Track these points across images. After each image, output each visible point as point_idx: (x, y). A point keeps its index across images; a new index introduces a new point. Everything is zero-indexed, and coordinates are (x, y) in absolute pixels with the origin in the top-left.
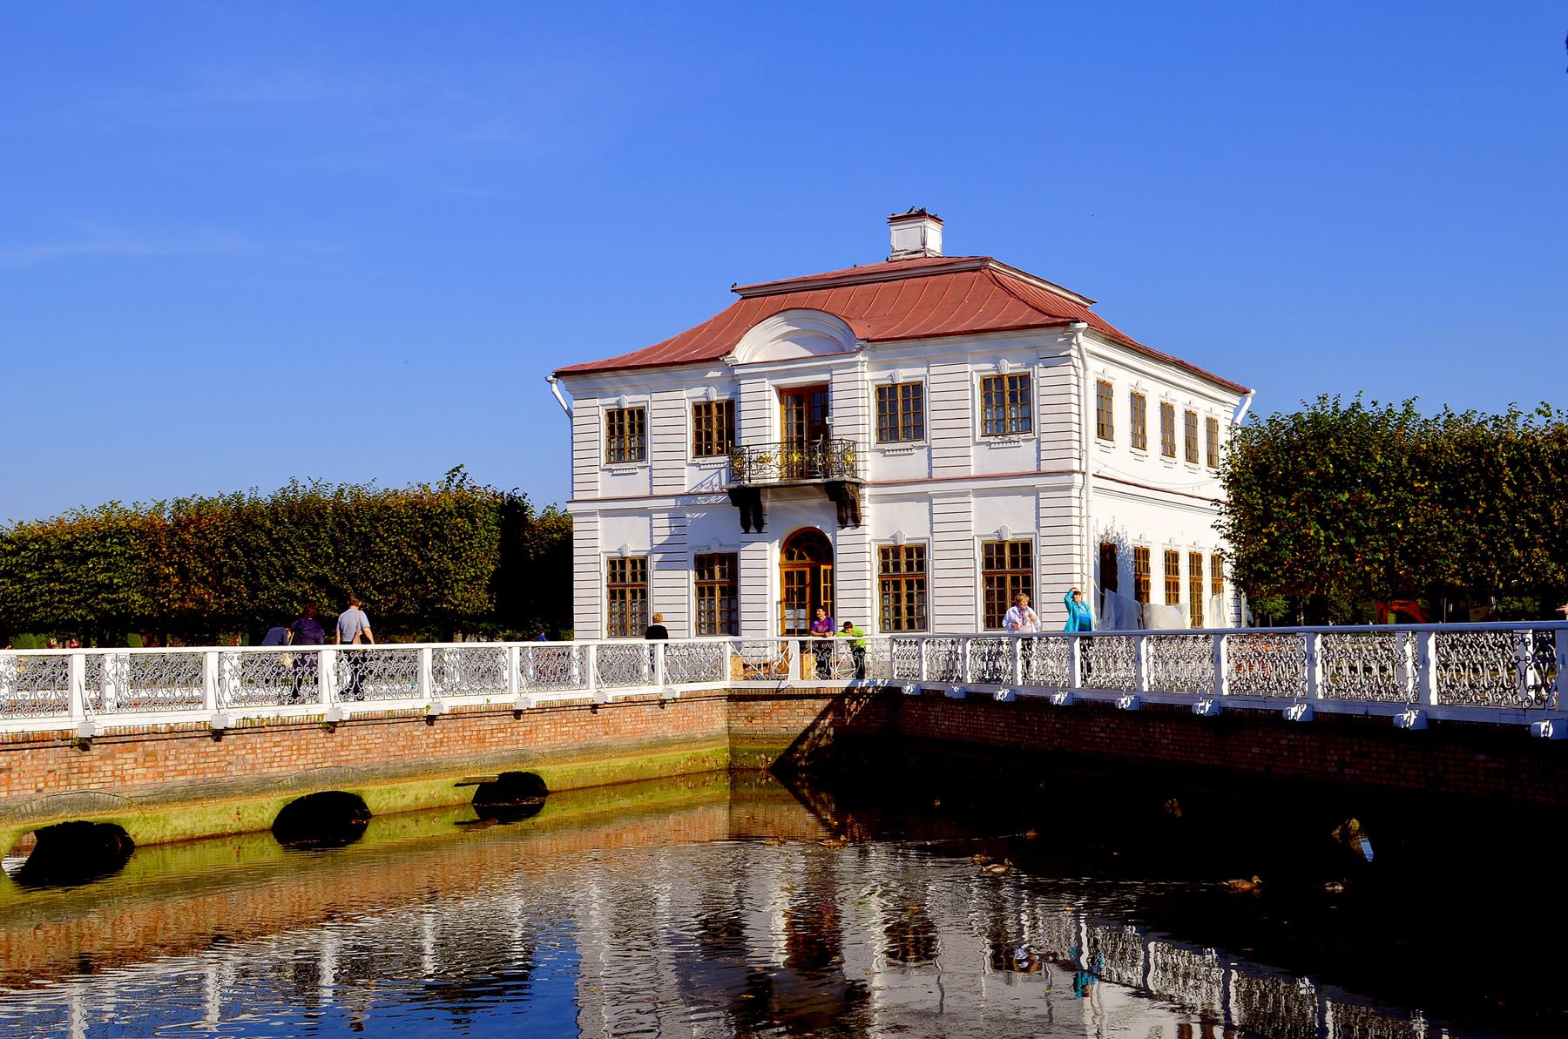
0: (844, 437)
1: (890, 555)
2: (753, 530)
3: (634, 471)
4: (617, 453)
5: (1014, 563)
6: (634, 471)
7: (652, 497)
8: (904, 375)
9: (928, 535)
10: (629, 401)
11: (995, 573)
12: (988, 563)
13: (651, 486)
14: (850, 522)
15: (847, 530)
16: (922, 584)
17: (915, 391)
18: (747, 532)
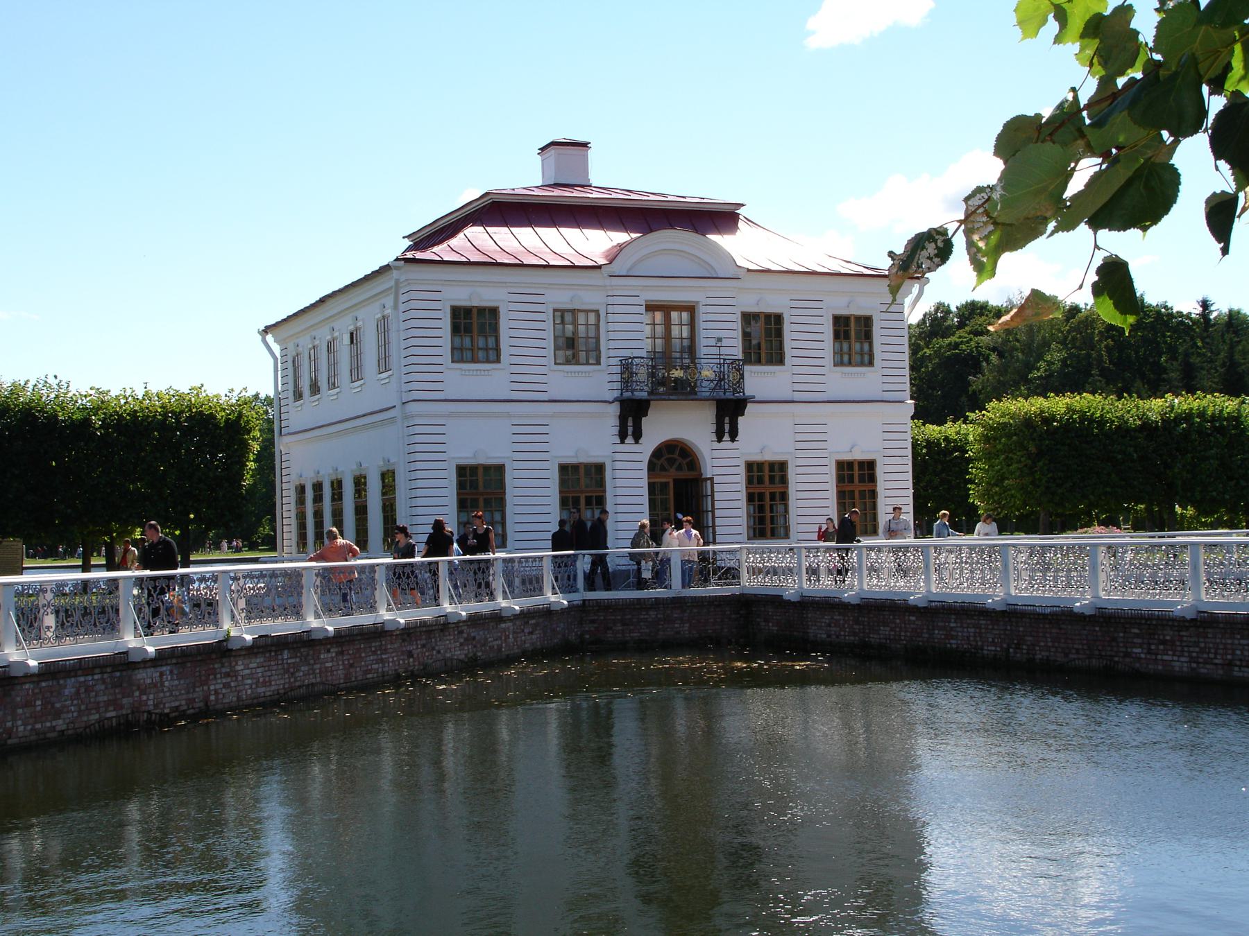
0: (726, 357)
2: (630, 440)
5: (862, 480)
12: (840, 479)
14: (727, 437)
18: (622, 442)
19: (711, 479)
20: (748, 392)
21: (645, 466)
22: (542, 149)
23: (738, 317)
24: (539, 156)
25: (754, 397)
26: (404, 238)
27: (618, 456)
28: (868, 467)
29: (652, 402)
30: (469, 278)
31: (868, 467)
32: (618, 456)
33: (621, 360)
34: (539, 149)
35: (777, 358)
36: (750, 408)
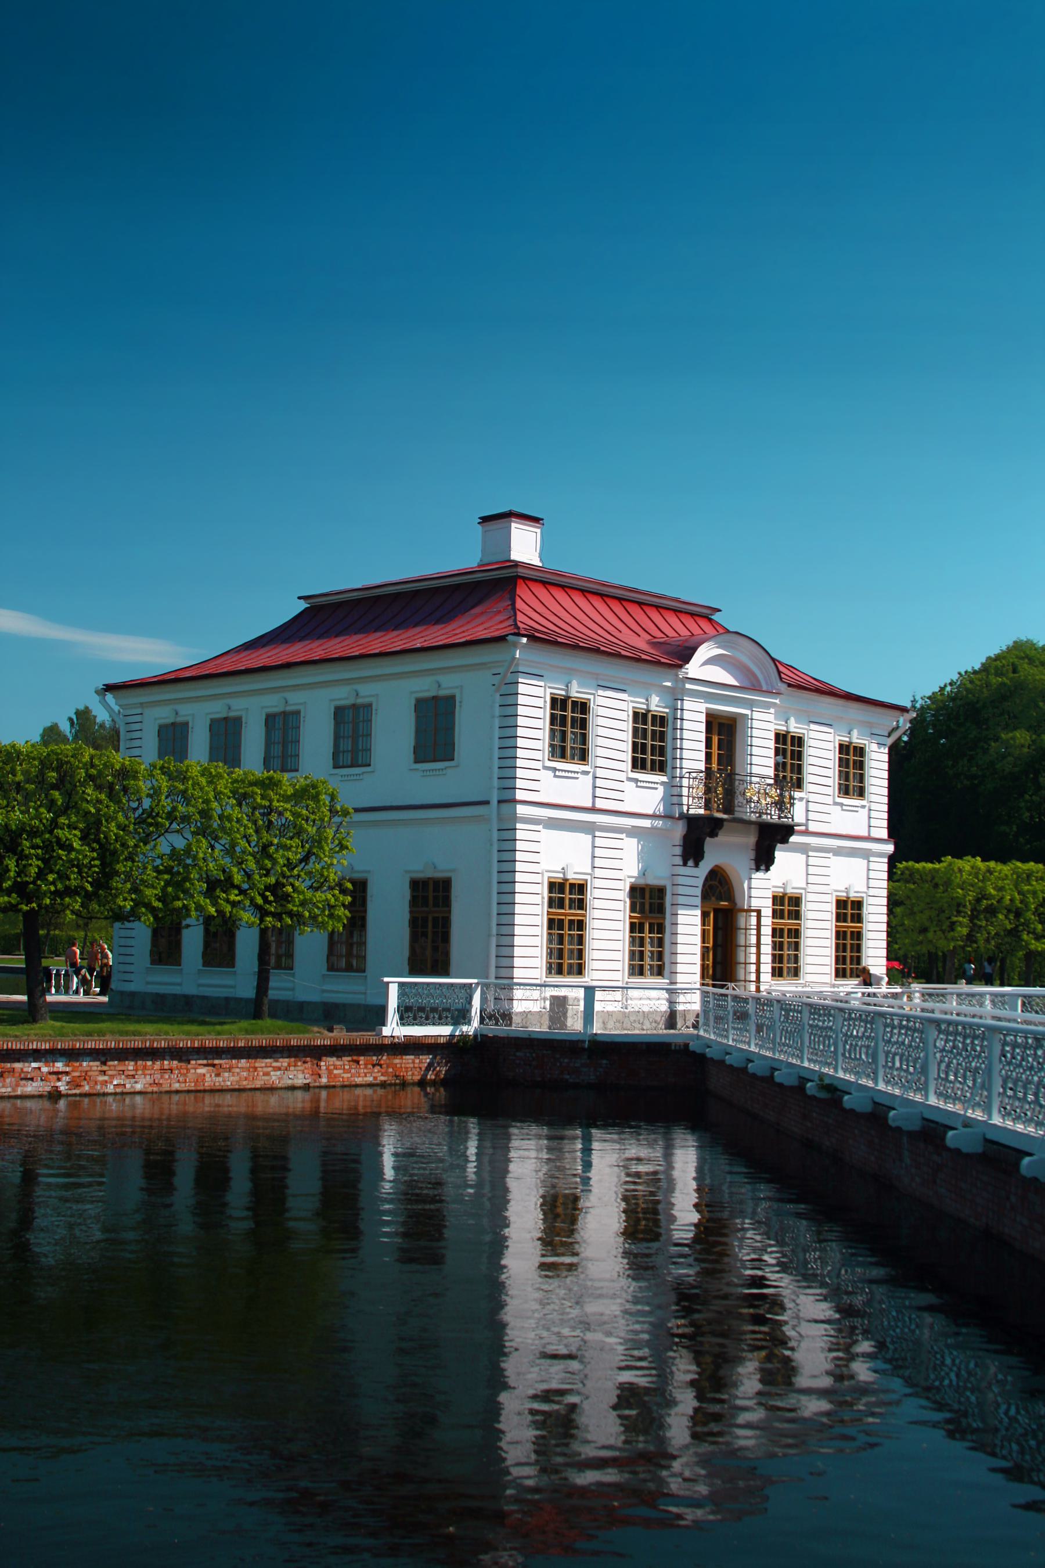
1: (778, 900)
2: (690, 863)
3: (576, 775)
4: (559, 751)
6: (576, 775)
7: (593, 810)
10: (577, 692)
13: (594, 797)
15: (760, 875)
16: (796, 933)
17: (799, 741)
18: (685, 864)
21: (698, 892)
22: (485, 520)
23: (772, 736)
24: (480, 527)
26: (300, 598)
27: (681, 880)
28: (858, 905)
30: (485, 659)
31: (858, 905)
32: (681, 880)
33: (690, 773)
34: (480, 518)
36: (793, 839)
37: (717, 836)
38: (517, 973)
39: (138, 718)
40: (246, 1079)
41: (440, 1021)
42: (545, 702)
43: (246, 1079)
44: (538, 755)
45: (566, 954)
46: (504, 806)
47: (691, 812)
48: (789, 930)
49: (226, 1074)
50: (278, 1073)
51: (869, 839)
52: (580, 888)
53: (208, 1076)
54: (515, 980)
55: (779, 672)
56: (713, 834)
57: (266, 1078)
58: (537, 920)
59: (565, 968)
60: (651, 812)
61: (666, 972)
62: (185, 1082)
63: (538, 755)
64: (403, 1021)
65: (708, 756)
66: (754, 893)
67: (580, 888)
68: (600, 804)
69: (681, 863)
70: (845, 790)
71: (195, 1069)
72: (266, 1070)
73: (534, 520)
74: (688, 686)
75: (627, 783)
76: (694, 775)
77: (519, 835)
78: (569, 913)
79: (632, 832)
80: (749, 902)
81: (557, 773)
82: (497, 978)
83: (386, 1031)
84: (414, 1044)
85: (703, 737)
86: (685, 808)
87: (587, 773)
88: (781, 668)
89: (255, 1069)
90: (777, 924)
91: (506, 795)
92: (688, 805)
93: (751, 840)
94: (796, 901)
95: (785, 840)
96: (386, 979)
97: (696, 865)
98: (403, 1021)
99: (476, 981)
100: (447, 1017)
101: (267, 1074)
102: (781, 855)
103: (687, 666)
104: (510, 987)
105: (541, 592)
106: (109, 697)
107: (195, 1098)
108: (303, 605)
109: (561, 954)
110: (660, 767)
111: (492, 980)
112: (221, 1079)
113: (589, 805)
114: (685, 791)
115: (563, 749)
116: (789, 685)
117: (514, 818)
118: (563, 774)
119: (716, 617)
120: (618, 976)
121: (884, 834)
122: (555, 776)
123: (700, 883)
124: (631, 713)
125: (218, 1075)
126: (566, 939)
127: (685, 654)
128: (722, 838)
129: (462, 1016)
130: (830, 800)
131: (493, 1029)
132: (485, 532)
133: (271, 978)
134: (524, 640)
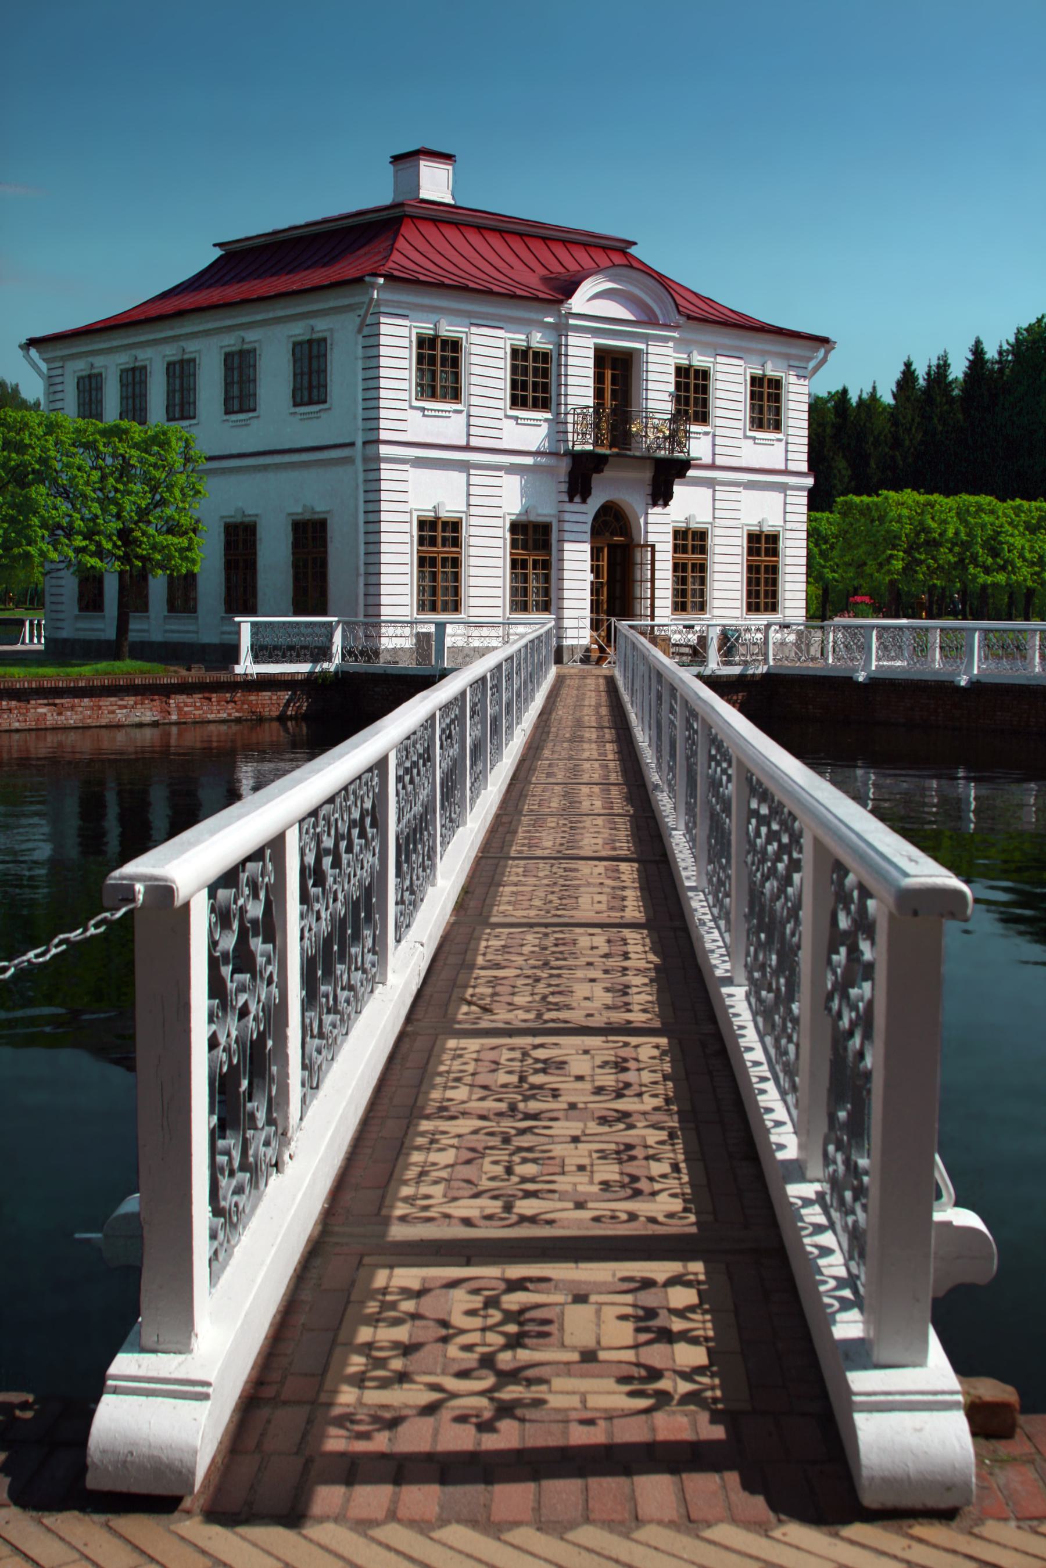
1: (680, 535)
2: (577, 499)
3: (447, 414)
6: (447, 414)
7: (468, 448)
8: (699, 360)
9: (782, 524)
10: (448, 329)
11: (438, 553)
13: (469, 435)
17: (704, 375)
18: (571, 500)
19: (653, 547)
20: (693, 454)
21: (588, 528)
22: (397, 159)
23: (672, 370)
24: (391, 167)
25: (700, 459)
26: (215, 245)
28: (774, 538)
29: (610, 459)
31: (774, 538)
35: (703, 418)
36: (691, 473)
37: (602, 471)
38: (384, 611)
39: (59, 372)
40: (90, 717)
41: (298, 659)
42: (411, 341)
43: (90, 717)
44: (405, 395)
45: (440, 592)
46: (368, 447)
47: (578, 448)
48: (693, 564)
49: (69, 713)
50: (124, 711)
51: (786, 472)
52: (455, 526)
53: (49, 715)
54: (383, 618)
55: (677, 305)
56: (600, 471)
57: (111, 716)
58: (407, 559)
59: (439, 604)
60: (534, 449)
61: (553, 608)
62: (26, 721)
63: (405, 395)
64: (257, 659)
65: (599, 394)
66: (650, 528)
67: (455, 526)
68: (474, 442)
69: (567, 499)
70: (758, 423)
71: (36, 708)
72: (110, 708)
73: (446, 157)
74: (572, 322)
75: (505, 420)
76: (579, 411)
77: (384, 475)
78: (441, 551)
79: (512, 469)
80: (646, 537)
81: (426, 413)
82: (365, 616)
83: (239, 669)
84: (270, 681)
85: (591, 373)
86: (570, 444)
87: (460, 412)
88: (679, 300)
89: (100, 707)
90: (679, 558)
91: (371, 437)
92: (573, 442)
93: (648, 475)
94: (701, 535)
95: (682, 475)
96: (237, 619)
97: (584, 501)
98: (257, 659)
99: (336, 619)
100: (305, 655)
101: (113, 712)
102: (679, 490)
103: (570, 301)
104: (378, 625)
105: (430, 231)
106: (33, 352)
107: (37, 737)
108: (218, 253)
109: (434, 591)
110: (543, 404)
111: (361, 618)
112: (63, 718)
113: (464, 443)
114: (570, 428)
115: (433, 388)
116: (689, 317)
117: (378, 459)
118: (433, 413)
119: (633, 251)
120: (406, 611)
121: (804, 467)
122: (424, 416)
123: (589, 519)
124: (509, 351)
125: (60, 714)
126: (440, 576)
127: (569, 289)
128: (608, 473)
129: (323, 653)
130: (739, 434)
131: (361, 666)
132: (396, 172)
133: (131, 621)
134: (381, 281)
